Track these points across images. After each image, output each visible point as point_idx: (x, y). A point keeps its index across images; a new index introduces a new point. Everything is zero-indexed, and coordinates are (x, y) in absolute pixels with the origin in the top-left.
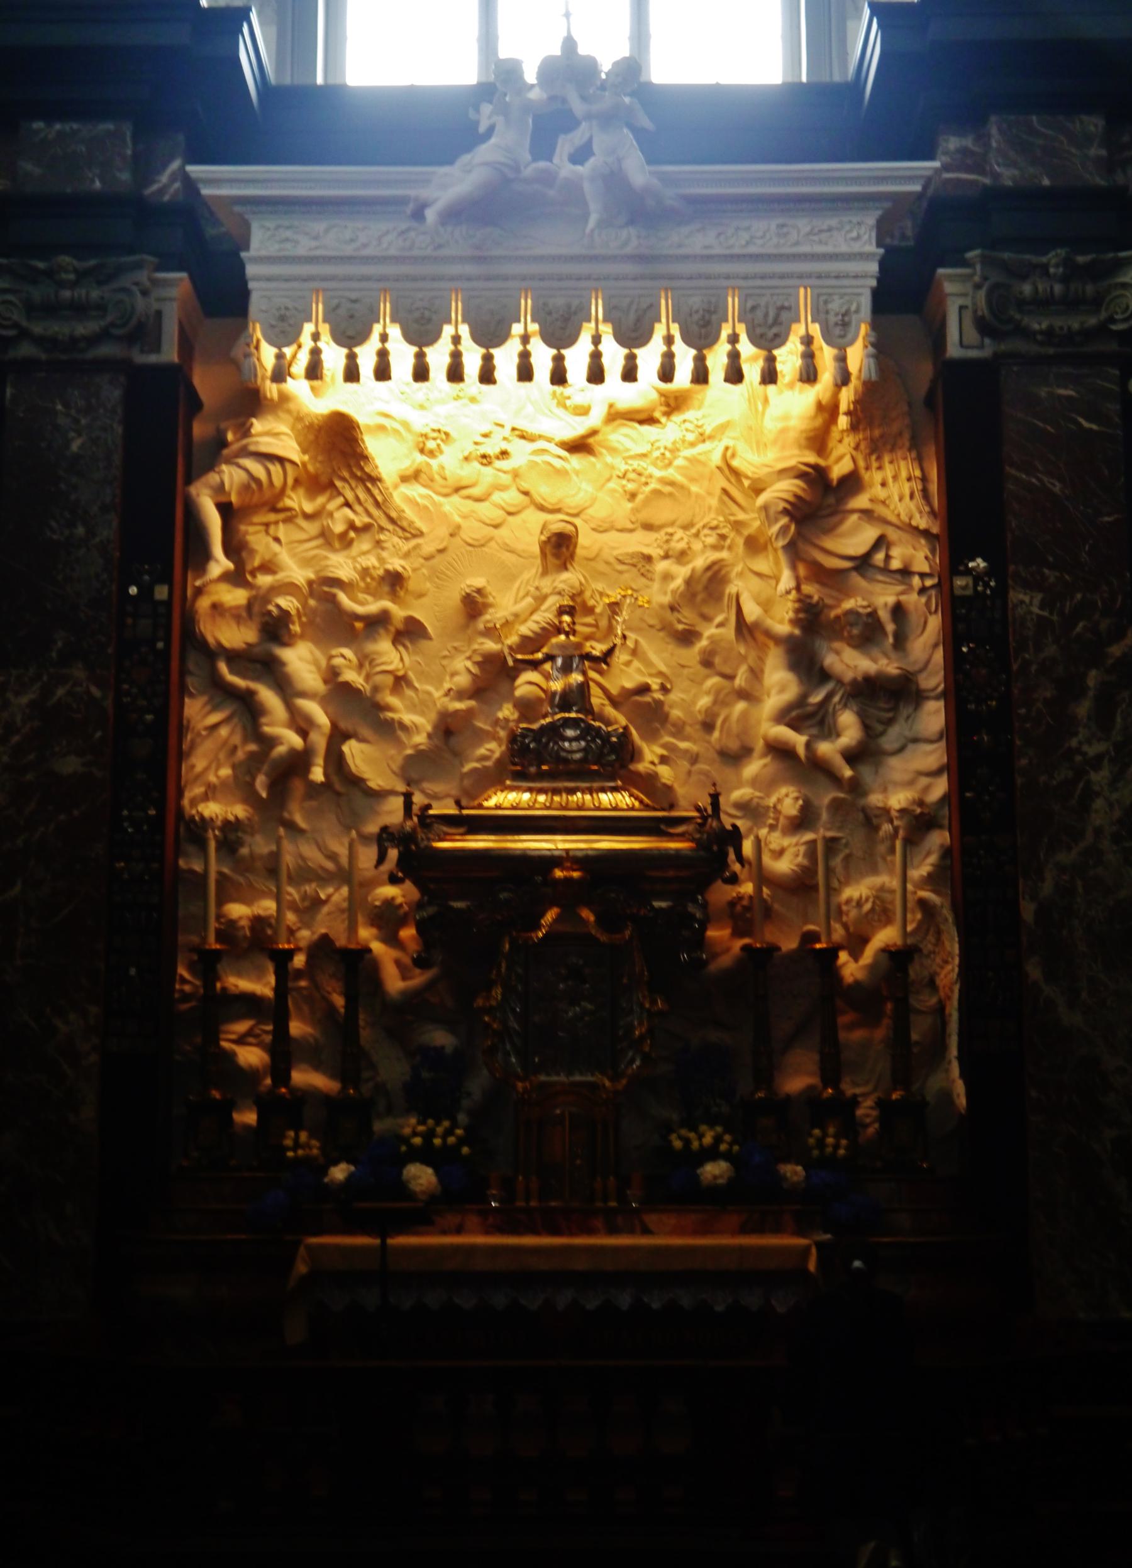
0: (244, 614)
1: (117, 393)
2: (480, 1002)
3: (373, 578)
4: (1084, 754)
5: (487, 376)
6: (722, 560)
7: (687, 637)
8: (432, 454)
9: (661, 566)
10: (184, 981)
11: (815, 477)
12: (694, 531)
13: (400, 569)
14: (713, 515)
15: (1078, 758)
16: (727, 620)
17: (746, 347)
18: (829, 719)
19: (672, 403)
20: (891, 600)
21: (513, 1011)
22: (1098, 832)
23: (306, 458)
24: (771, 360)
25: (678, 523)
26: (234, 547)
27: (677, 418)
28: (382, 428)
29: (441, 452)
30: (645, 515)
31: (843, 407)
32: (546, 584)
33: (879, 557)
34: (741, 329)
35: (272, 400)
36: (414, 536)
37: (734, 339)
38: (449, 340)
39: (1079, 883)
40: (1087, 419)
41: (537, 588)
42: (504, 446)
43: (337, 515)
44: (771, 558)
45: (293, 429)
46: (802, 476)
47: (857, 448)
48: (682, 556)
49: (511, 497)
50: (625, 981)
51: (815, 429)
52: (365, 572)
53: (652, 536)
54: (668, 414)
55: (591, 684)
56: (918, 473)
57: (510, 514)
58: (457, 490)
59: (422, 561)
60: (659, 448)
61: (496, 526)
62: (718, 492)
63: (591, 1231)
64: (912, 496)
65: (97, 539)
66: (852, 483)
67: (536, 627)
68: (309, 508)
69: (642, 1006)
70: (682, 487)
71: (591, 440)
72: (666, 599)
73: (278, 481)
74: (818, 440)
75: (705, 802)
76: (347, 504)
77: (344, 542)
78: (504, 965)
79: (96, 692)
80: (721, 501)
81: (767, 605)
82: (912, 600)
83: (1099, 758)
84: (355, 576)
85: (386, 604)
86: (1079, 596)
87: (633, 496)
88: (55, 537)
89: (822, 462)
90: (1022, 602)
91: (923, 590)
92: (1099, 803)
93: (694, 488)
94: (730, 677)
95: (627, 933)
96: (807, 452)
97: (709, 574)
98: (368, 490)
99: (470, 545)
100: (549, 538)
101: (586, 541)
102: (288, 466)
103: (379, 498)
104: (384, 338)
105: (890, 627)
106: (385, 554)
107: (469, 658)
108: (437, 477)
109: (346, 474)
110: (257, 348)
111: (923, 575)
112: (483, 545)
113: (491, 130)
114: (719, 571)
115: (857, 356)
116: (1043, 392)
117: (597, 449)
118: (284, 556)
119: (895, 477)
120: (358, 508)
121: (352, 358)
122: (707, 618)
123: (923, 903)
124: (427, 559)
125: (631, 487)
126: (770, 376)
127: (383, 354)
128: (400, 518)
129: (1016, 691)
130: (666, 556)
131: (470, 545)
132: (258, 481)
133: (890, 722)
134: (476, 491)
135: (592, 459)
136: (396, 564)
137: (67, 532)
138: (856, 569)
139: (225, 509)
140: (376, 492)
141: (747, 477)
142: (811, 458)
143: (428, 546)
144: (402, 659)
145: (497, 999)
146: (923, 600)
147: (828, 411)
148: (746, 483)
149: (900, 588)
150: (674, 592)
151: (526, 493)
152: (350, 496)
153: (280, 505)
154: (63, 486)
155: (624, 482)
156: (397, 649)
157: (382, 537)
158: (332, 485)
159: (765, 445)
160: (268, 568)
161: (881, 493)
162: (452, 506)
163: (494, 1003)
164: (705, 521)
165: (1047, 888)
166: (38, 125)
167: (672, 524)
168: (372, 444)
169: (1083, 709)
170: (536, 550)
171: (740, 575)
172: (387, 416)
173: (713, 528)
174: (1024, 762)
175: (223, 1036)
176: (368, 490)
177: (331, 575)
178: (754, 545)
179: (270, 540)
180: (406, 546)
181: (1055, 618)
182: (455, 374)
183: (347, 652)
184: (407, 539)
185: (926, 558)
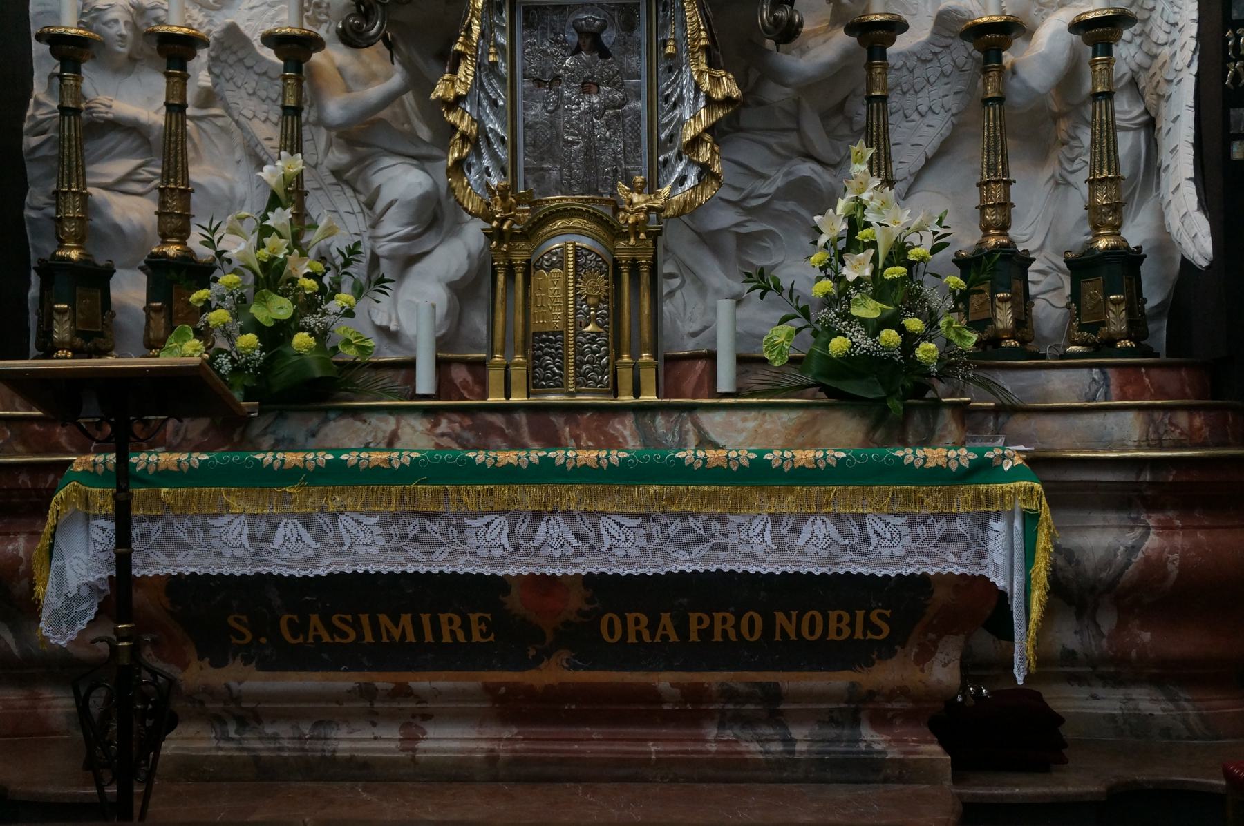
2: (440, 91)
10: (38, 104)
21: (494, 103)
69: (697, 88)
78: (476, 29)
145: (465, 83)
163: (462, 92)
175: (89, 180)
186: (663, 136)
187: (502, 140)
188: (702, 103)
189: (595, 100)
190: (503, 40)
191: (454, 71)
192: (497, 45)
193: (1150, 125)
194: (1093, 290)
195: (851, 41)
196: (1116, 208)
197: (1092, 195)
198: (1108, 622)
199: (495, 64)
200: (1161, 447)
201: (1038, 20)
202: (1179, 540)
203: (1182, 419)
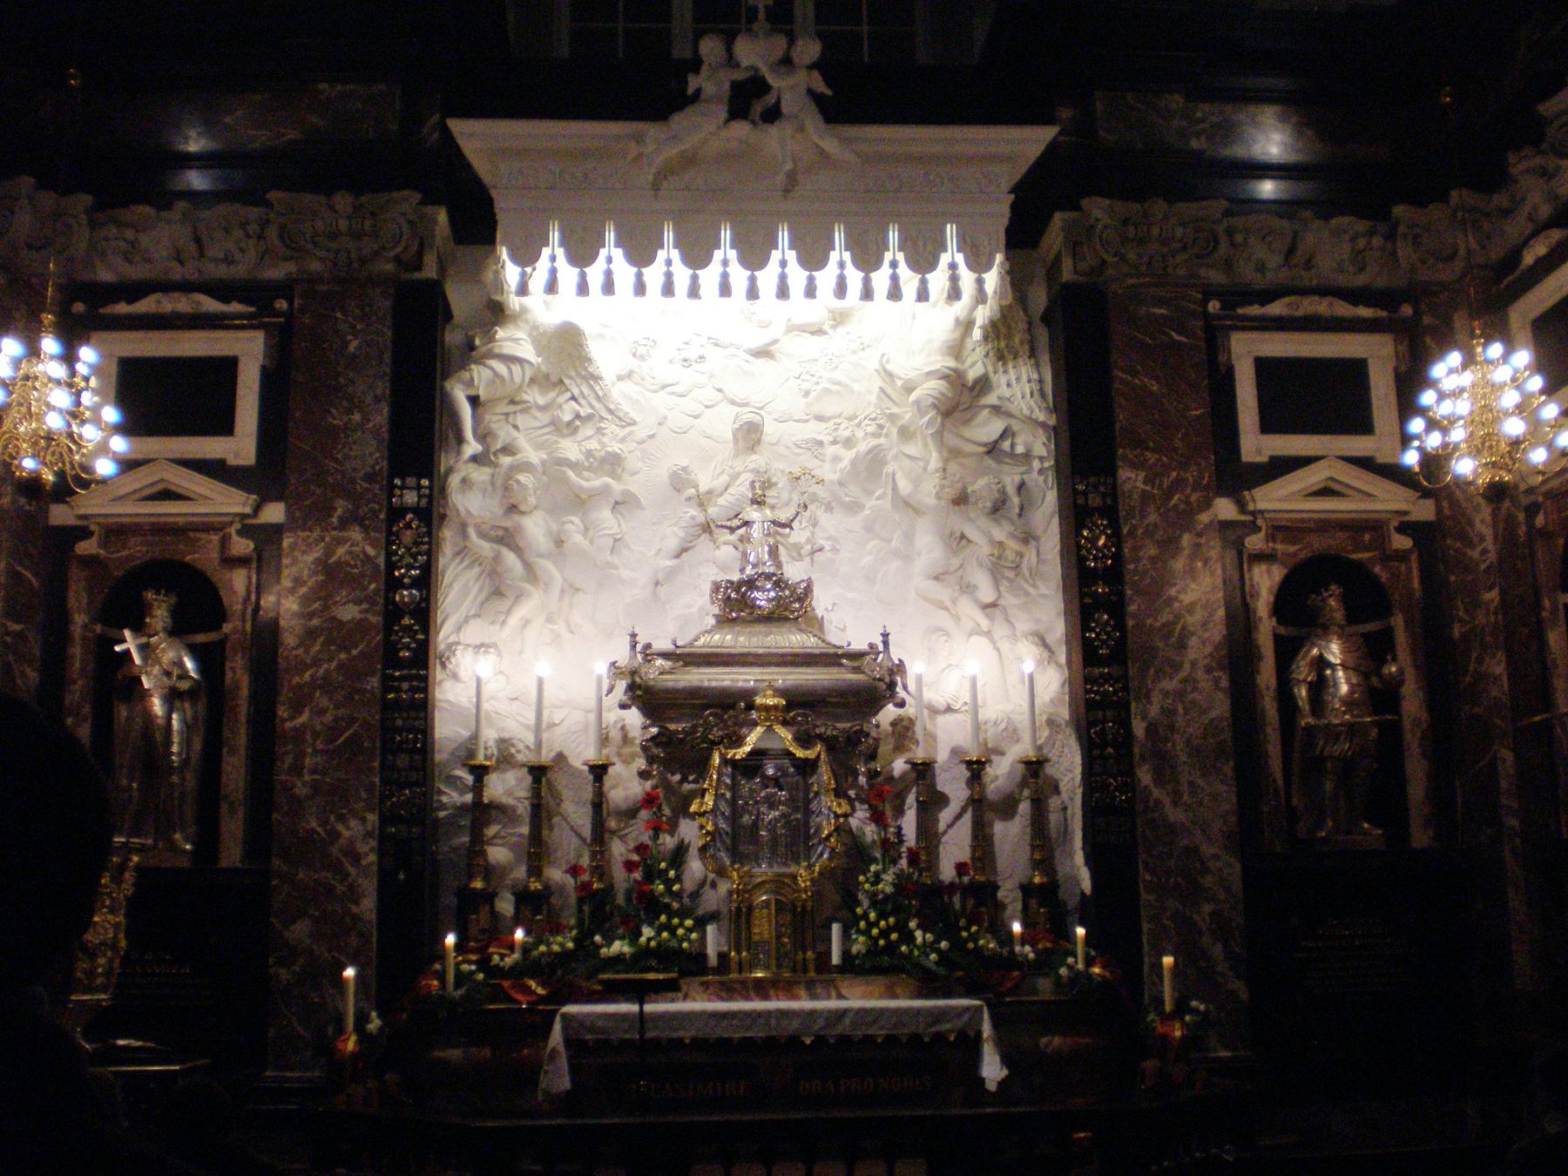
0: (490, 488)
1: (388, 304)
3: (595, 458)
5: (694, 292)
6: (880, 445)
7: (853, 508)
8: (642, 358)
9: (831, 450)
11: (955, 378)
12: (857, 421)
13: (619, 451)
14: (872, 409)
15: (1176, 605)
16: (885, 493)
17: (904, 271)
19: (838, 317)
20: (1017, 479)
22: (1193, 664)
23: (540, 359)
24: (924, 282)
25: (844, 415)
26: (483, 436)
27: (840, 330)
28: (601, 336)
29: (650, 357)
30: (817, 409)
31: (979, 322)
32: (739, 465)
33: (1006, 445)
34: (900, 257)
35: (515, 310)
36: (629, 424)
37: (894, 264)
38: (663, 263)
40: (1179, 333)
41: (731, 467)
42: (701, 352)
43: (564, 407)
44: (920, 443)
45: (530, 335)
46: (945, 377)
47: (987, 355)
48: (848, 443)
49: (709, 395)
50: (815, 789)
51: (954, 341)
52: (589, 454)
53: (824, 425)
54: (834, 327)
55: (780, 547)
56: (1035, 376)
57: (707, 407)
58: (663, 387)
59: (635, 445)
60: (827, 355)
61: (696, 417)
62: (876, 390)
63: (795, 998)
64: (1032, 394)
65: (371, 425)
66: (983, 385)
67: (731, 499)
68: (541, 401)
70: (847, 386)
71: (772, 348)
72: (836, 477)
73: (518, 379)
74: (956, 349)
75: (878, 641)
76: (573, 398)
77: (571, 429)
78: (715, 777)
79: (371, 552)
80: (879, 397)
81: (917, 482)
82: (1034, 479)
84: (581, 457)
85: (609, 480)
86: (1174, 474)
87: (807, 393)
88: (335, 422)
89: (959, 366)
90: (1129, 479)
91: (1041, 472)
92: (1193, 642)
93: (856, 387)
94: (889, 541)
95: (818, 748)
96: (948, 358)
97: (871, 455)
98: (591, 387)
99: (675, 432)
100: (741, 425)
101: (771, 430)
102: (526, 366)
103: (600, 393)
104: (609, 260)
105: (1016, 500)
106: (605, 439)
107: (675, 524)
108: (647, 377)
109: (573, 374)
110: (503, 267)
111: (1041, 459)
112: (685, 433)
113: (698, 91)
114: (879, 453)
115: (992, 279)
116: (1142, 311)
117: (777, 355)
118: (522, 441)
119: (1018, 379)
120: (582, 401)
121: (583, 276)
122: (869, 493)
124: (639, 443)
125: (806, 386)
126: (923, 295)
127: (609, 274)
128: (618, 409)
129: (1126, 550)
130: (835, 442)
131: (675, 432)
132: (501, 377)
134: (678, 389)
135: (772, 362)
136: (615, 447)
137: (345, 419)
139: (474, 401)
140: (597, 388)
141: (900, 379)
142: (952, 363)
143: (641, 432)
144: (619, 525)
146: (1042, 478)
147: (967, 325)
148: (899, 383)
149: (1023, 469)
150: (842, 471)
151: (720, 390)
152: (576, 392)
153: (517, 399)
154: (341, 380)
155: (799, 381)
156: (617, 518)
157: (602, 425)
158: (561, 382)
159: (914, 352)
160: (508, 450)
161: (1006, 393)
162: (661, 401)
164: (867, 413)
165: (1154, 710)
166: (323, 86)
167: (839, 416)
168: (595, 349)
170: (730, 436)
171: (895, 457)
172: (606, 326)
173: (874, 419)
174: (1133, 608)
176: (591, 387)
177: (561, 455)
178: (905, 434)
179: (511, 427)
180: (622, 433)
182: (668, 289)
183: (573, 518)
184: (623, 427)
185: (1044, 444)
186: (812, 831)
187: (727, 833)
188: (832, 816)
189: (777, 813)
190: (728, 781)
191: (703, 796)
192: (726, 784)
195: (908, 766)
197: (1032, 854)
199: (723, 795)
201: (1006, 749)
202: (1069, 1040)
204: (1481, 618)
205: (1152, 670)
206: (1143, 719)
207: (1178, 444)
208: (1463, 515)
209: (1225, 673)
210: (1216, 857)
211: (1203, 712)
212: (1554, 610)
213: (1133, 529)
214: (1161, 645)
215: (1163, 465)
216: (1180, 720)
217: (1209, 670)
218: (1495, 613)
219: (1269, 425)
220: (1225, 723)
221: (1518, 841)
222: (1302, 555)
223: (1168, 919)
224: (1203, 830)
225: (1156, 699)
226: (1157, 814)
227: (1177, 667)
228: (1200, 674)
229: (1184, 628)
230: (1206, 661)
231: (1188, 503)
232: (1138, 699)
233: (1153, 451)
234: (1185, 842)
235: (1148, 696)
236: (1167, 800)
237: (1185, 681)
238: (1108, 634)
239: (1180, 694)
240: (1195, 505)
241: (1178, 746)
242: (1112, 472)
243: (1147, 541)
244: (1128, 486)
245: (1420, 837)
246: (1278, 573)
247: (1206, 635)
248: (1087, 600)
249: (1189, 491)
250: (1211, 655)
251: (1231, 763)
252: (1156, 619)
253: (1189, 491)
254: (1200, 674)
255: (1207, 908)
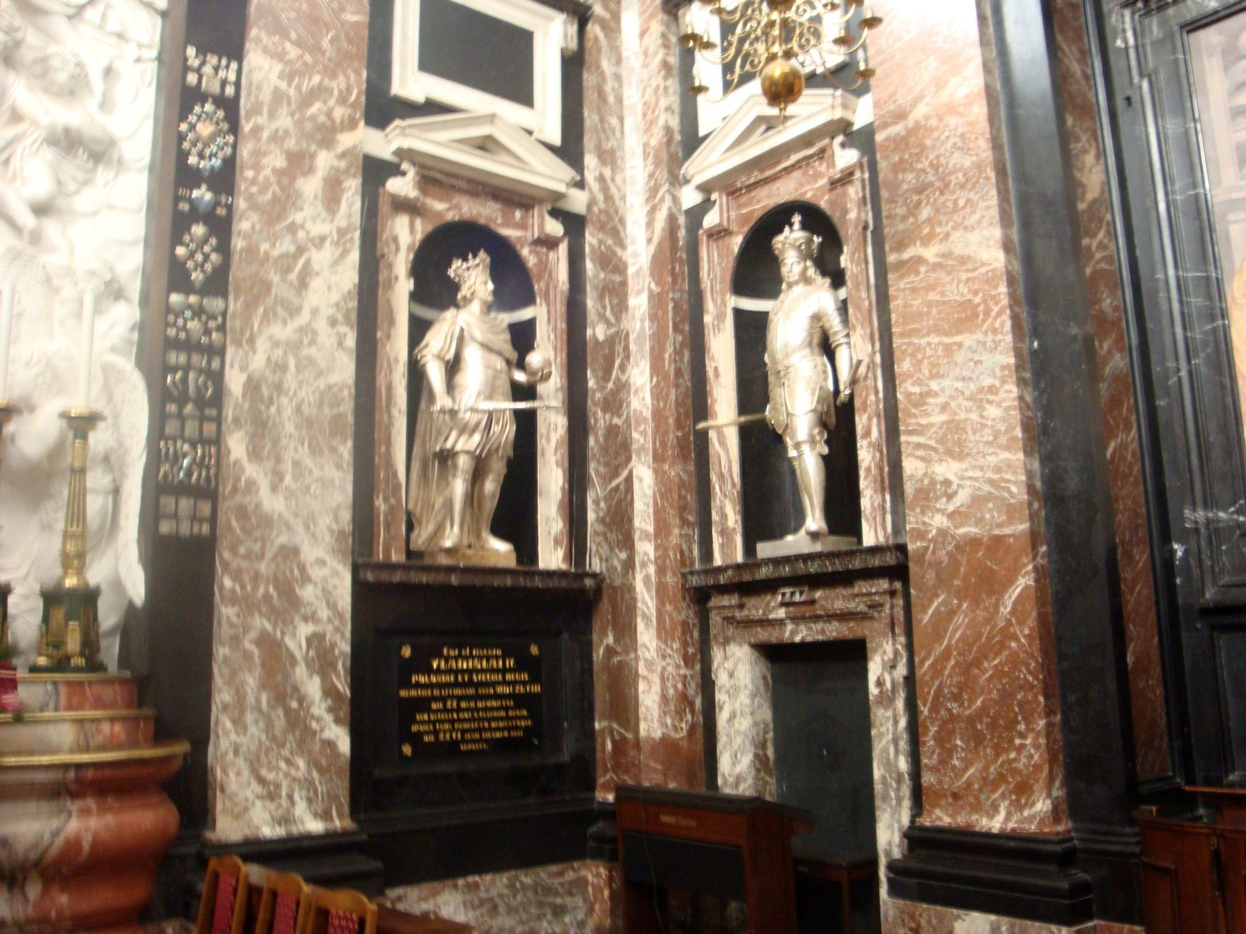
4: (308, 233)
15: (301, 234)
18: (15, 163)
20: (104, 63)
39: (292, 363)
82: (125, 67)
83: (323, 239)
86: (316, 79)
91: (138, 60)
92: (316, 284)
111: (140, 46)
123: (107, 369)
133: (86, 183)
138: (70, 18)
165: (258, 362)
169: (311, 186)
181: (292, 92)
193: (116, 491)
194: (59, 614)
196: (81, 556)
198: (34, 890)
200: (87, 749)
203: (106, 728)
204: (625, 324)
205: (261, 310)
206: (243, 368)
207: (325, 43)
208: (616, 212)
209: (352, 327)
210: (321, 563)
211: (320, 374)
212: (720, 317)
213: (257, 130)
214: (276, 279)
215: (305, 64)
216: (290, 381)
217: (333, 322)
218: (642, 322)
219: (430, 62)
220: (346, 393)
221: (652, 569)
222: (451, 216)
223: (251, 642)
224: (307, 527)
225: (262, 345)
226: (247, 499)
227: (294, 311)
228: (322, 325)
229: (308, 263)
230: (332, 311)
231: (329, 114)
232: (238, 344)
233: (293, 43)
234: (283, 539)
235: (252, 341)
236: (264, 484)
237: (302, 330)
238: (206, 257)
239: (295, 347)
240: (338, 121)
241: (285, 414)
242: (235, 52)
243: (272, 147)
244: (257, 76)
245: (551, 557)
246: (421, 229)
247: (334, 279)
248: (184, 207)
249: (332, 102)
250: (337, 305)
251: (350, 443)
252: (273, 245)
253: (332, 102)
254: (322, 325)
255: (305, 630)
